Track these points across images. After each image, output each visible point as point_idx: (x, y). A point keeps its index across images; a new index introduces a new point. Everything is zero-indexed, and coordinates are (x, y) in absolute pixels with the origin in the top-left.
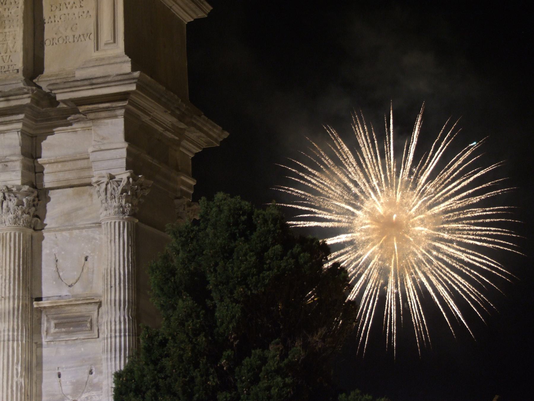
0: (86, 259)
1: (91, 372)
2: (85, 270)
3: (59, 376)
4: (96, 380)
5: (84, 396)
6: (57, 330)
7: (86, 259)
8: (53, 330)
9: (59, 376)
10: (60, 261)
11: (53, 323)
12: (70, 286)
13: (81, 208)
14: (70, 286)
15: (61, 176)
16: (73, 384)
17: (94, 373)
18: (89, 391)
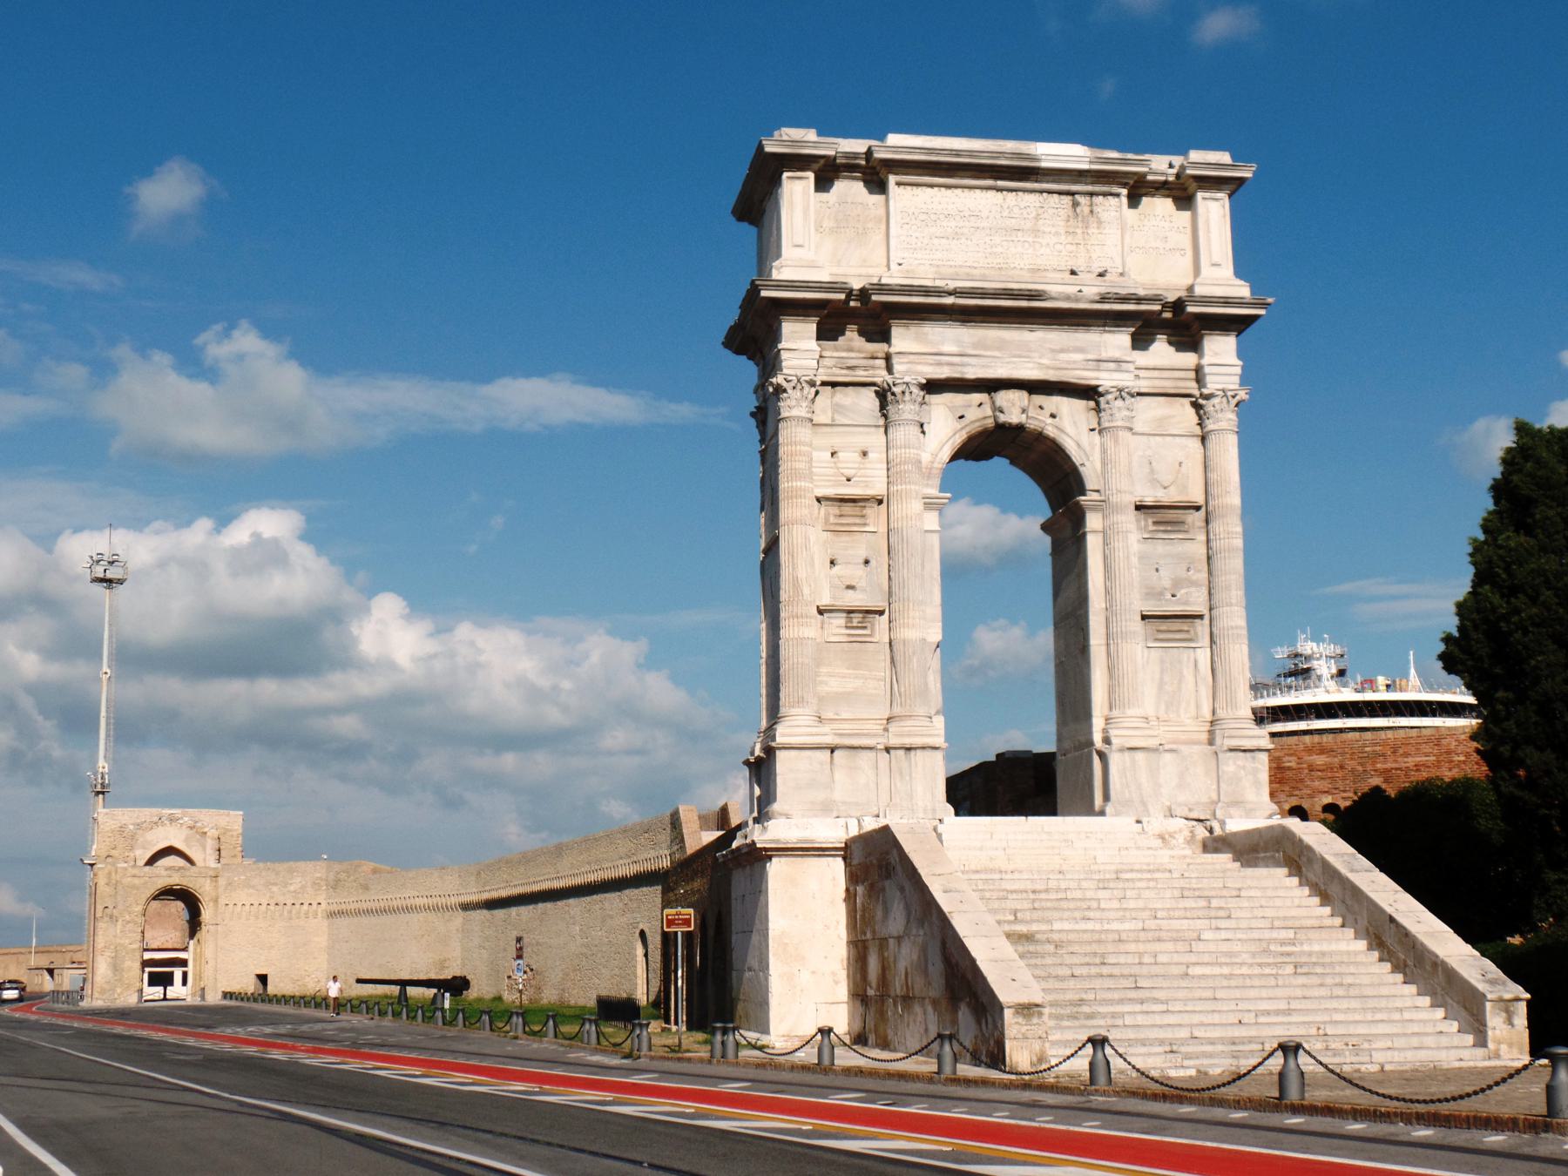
0: (1180, 464)
1: (1188, 570)
2: (1180, 475)
3: (1157, 570)
4: (1194, 578)
5: (1183, 591)
6: (1154, 528)
7: (1180, 464)
8: (1152, 528)
9: (1157, 570)
10: (1154, 464)
11: (1150, 521)
12: (1165, 488)
13: (1174, 416)
14: (1165, 488)
15: (1158, 383)
16: (1172, 579)
17: (1192, 572)
18: (1188, 587)
